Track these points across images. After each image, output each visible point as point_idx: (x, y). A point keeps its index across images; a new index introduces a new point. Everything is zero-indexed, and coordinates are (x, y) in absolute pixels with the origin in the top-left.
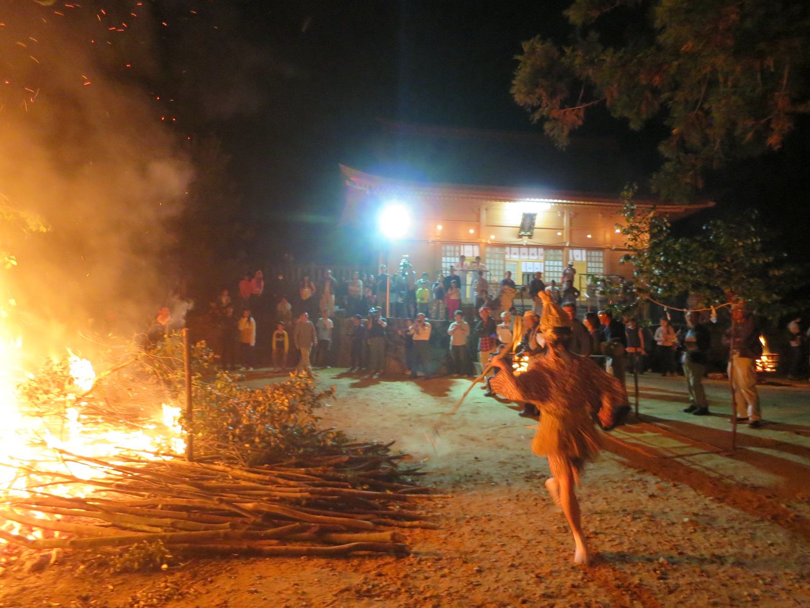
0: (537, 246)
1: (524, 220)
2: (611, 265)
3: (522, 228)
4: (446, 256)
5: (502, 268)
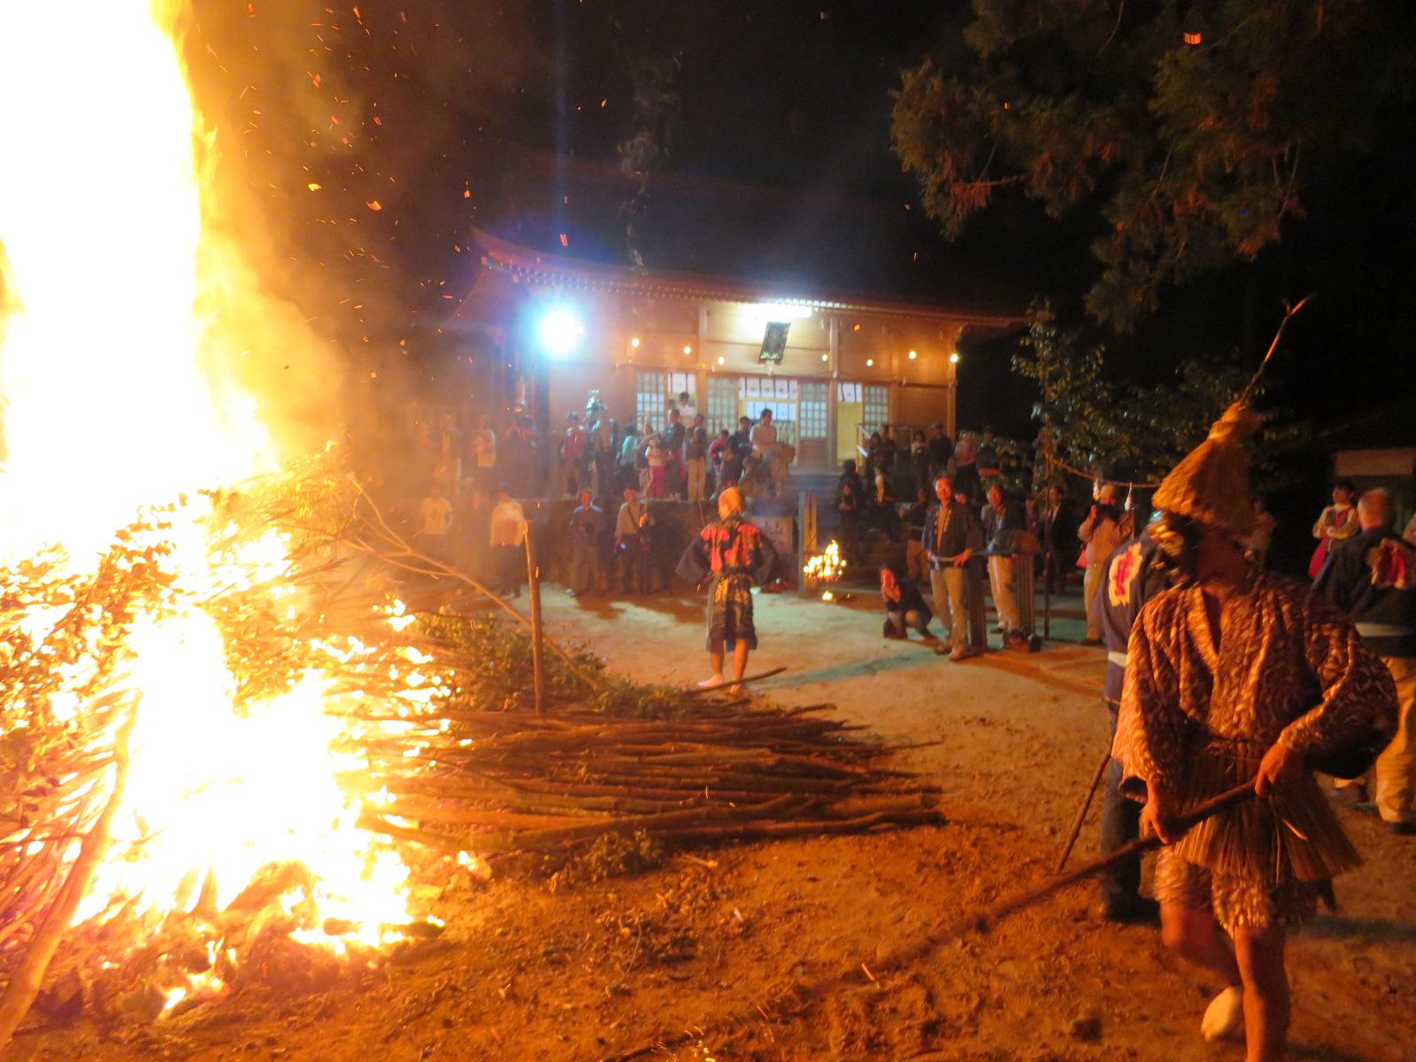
0: (788, 378)
1: (769, 333)
2: (900, 407)
3: (766, 346)
4: (643, 391)
5: (733, 412)
